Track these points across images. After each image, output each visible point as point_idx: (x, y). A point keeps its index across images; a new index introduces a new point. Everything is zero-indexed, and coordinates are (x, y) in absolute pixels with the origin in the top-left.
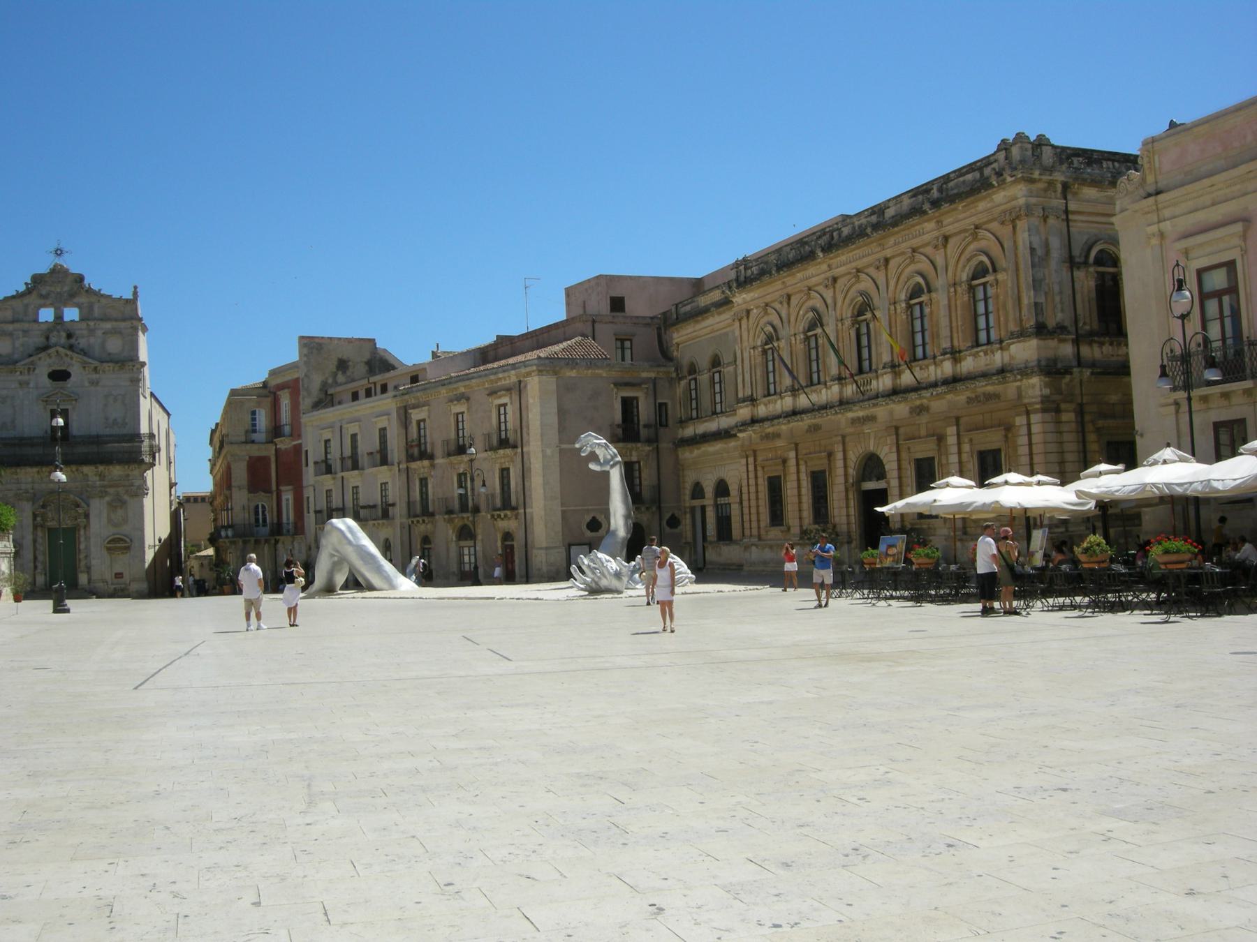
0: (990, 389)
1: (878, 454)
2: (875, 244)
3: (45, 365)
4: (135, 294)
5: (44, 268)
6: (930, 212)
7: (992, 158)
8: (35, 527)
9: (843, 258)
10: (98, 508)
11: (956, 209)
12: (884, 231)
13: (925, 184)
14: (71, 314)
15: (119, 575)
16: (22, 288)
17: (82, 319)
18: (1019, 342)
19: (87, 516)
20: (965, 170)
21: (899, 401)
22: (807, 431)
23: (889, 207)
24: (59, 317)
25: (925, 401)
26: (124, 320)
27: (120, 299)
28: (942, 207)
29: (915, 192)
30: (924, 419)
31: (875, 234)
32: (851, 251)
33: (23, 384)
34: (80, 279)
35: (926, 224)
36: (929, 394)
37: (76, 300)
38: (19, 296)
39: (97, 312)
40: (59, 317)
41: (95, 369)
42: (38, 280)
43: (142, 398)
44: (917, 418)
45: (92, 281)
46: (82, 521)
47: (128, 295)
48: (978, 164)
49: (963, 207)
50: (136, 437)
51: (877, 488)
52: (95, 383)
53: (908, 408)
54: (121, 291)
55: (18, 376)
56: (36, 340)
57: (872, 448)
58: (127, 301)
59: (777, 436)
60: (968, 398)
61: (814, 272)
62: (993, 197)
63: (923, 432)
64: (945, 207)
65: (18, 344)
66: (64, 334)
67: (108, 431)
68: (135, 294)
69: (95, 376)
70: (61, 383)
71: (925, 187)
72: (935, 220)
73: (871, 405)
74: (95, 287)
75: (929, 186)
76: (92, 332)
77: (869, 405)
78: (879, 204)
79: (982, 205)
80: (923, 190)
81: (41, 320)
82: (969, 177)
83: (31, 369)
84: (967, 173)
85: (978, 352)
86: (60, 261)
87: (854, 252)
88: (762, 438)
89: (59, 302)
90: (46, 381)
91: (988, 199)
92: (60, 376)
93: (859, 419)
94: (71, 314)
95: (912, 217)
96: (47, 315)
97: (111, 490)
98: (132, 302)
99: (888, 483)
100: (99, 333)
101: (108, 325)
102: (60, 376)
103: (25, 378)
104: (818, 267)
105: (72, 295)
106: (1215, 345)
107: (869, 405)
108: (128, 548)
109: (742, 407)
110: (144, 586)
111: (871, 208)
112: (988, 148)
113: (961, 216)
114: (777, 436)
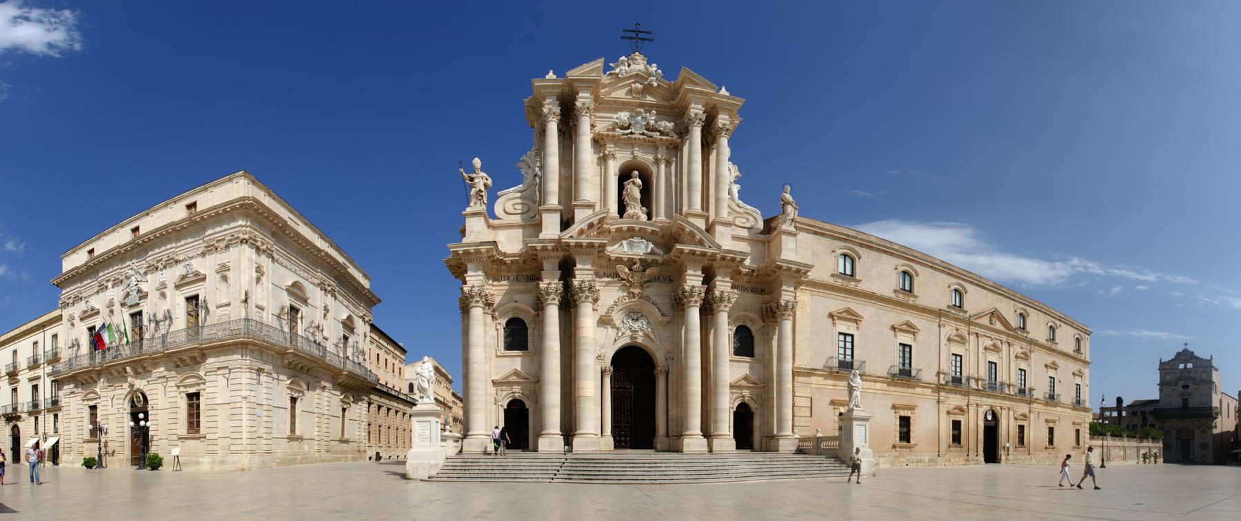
3: (1180, 385)
4: (1211, 357)
5: (1180, 350)
8: (1177, 438)
10: (1197, 432)
14: (1190, 366)
15: (1204, 456)
16: (1173, 357)
17: (1194, 367)
19: (1193, 434)
24: (1185, 366)
26: (1207, 367)
27: (1206, 360)
33: (1174, 390)
34: (1193, 353)
37: (1192, 360)
38: (1172, 360)
39: (1198, 365)
40: (1185, 366)
41: (1197, 384)
42: (1178, 354)
43: (1214, 395)
45: (1197, 354)
46: (1192, 437)
47: (1209, 358)
50: (1211, 408)
52: (1197, 389)
54: (1205, 356)
55: (1172, 387)
56: (1178, 375)
58: (1209, 360)
65: (1172, 376)
66: (1187, 373)
67: (1202, 406)
68: (1211, 357)
69: (1197, 387)
70: (1185, 390)
74: (1198, 356)
76: (1196, 372)
81: (1180, 368)
83: (1176, 384)
86: (1186, 347)
89: (1185, 362)
90: (1181, 389)
92: (1186, 387)
94: (1190, 366)
96: (1181, 366)
97: (1202, 427)
98: (1210, 361)
100: (1199, 372)
101: (1202, 369)
102: (1186, 387)
103: (1175, 387)
105: (1190, 359)
108: (1207, 447)
110: (1212, 460)
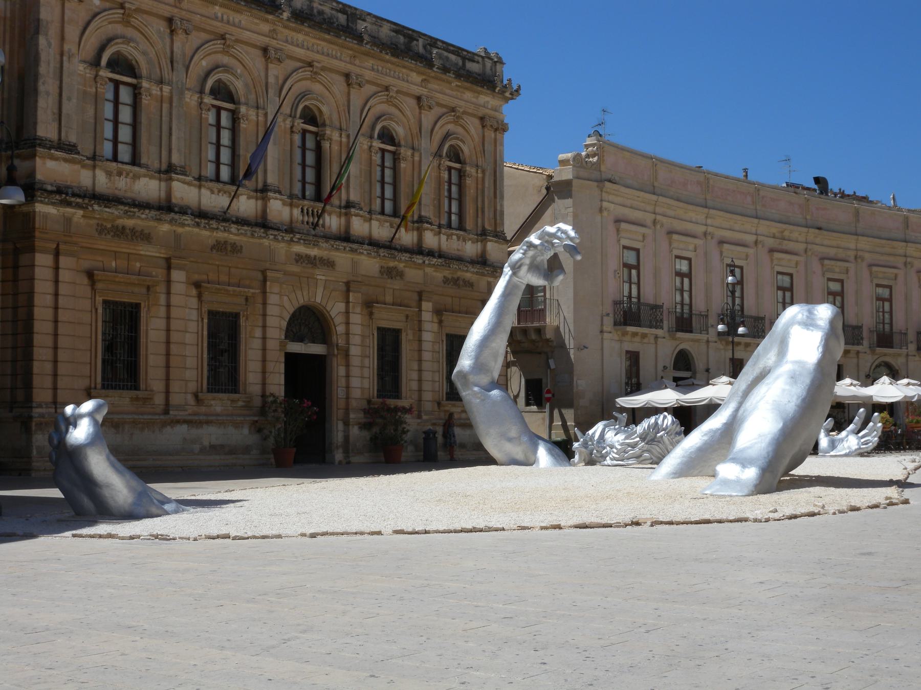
0: (468, 275)
1: (329, 309)
2: (350, 52)
6: (435, 69)
7: (476, 57)
9: (300, 37)
11: (450, 83)
12: (381, 52)
13: (413, 31)
18: (496, 242)
20: (452, 48)
21: (384, 256)
22: (213, 248)
23: (364, 20)
25: (401, 265)
28: (448, 74)
29: (399, 29)
30: (397, 284)
31: (368, 46)
32: (319, 39)
35: (415, 74)
36: (421, 261)
44: (389, 281)
48: (465, 53)
49: (457, 86)
51: (303, 352)
53: (377, 268)
57: (318, 300)
59: (145, 237)
60: (444, 277)
61: (243, 22)
62: (481, 96)
63: (389, 299)
64: (450, 76)
71: (410, 32)
72: (424, 77)
73: (348, 249)
75: (415, 35)
77: (345, 249)
78: (356, 9)
79: (468, 95)
80: (411, 35)
82: (453, 57)
84: (453, 52)
85: (452, 234)
87: (319, 42)
88: (101, 230)
91: (476, 94)
93: (308, 256)
95: (416, 61)
99: (283, 345)
104: (256, 21)
106: (633, 300)
107: (345, 249)
109: (53, 158)
111: (345, 5)
112: (477, 49)
113: (448, 91)
114: (145, 237)
